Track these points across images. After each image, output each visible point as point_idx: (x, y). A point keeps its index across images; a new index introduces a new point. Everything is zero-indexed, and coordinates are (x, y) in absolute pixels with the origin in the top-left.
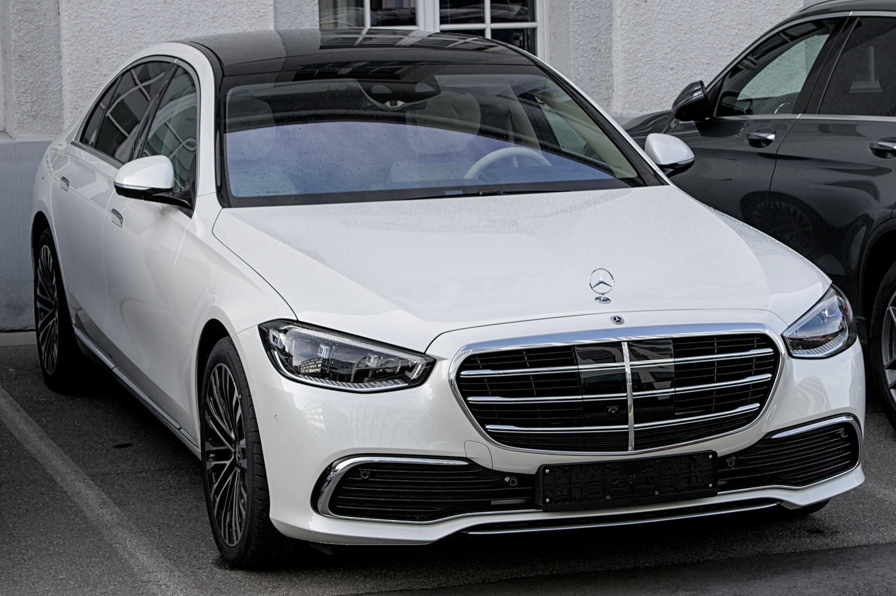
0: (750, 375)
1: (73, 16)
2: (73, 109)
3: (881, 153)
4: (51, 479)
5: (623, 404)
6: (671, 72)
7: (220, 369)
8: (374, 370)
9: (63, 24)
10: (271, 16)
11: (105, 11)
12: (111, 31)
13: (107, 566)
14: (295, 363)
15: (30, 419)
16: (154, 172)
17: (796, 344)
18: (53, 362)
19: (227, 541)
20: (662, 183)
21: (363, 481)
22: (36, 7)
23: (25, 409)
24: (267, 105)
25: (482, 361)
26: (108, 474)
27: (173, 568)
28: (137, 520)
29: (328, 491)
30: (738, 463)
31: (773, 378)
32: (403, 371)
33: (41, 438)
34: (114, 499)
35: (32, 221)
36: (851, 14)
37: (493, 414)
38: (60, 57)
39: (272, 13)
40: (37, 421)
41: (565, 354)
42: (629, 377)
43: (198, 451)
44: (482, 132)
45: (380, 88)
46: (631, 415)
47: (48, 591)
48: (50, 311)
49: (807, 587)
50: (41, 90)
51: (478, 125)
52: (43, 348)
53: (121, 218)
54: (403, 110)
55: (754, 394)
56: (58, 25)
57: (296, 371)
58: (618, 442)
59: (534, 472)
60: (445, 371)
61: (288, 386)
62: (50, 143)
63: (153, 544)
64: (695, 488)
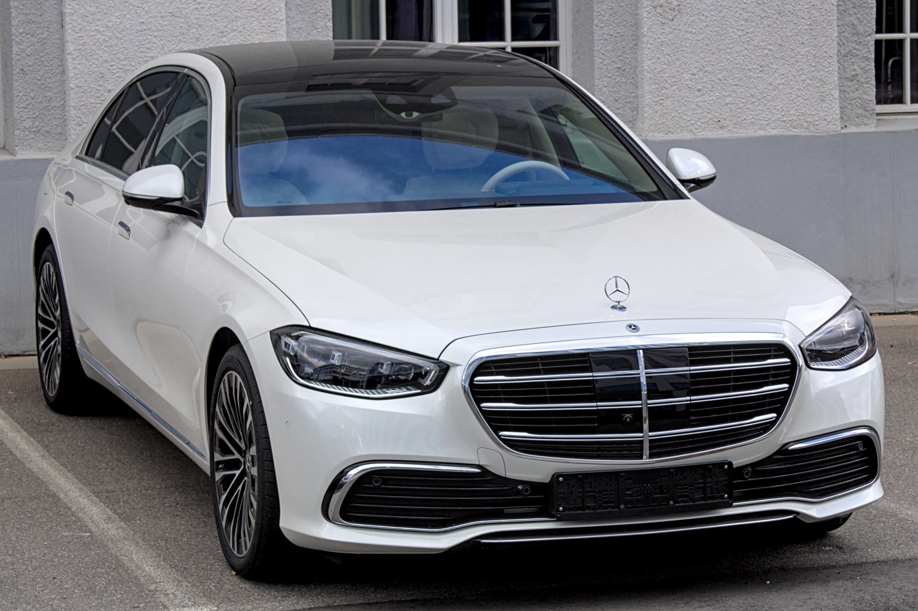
0: (767, 384)
2: (76, 125)
4: (54, 495)
6: (698, 94)
9: (68, 38)
11: (110, 24)
13: (113, 576)
15: (32, 439)
16: (167, 181)
19: (236, 552)
20: (681, 196)
21: (375, 488)
22: (39, 19)
23: (25, 430)
24: (278, 118)
26: (113, 492)
28: (144, 534)
29: (338, 498)
30: (755, 473)
32: (414, 376)
33: (43, 457)
34: (119, 515)
35: (34, 238)
37: (506, 421)
39: (284, 28)
40: (39, 442)
43: (205, 463)
44: (499, 148)
45: (395, 99)
47: (55, 599)
48: (52, 331)
50: (44, 105)
53: (128, 230)
55: (770, 404)
56: (62, 39)
57: (308, 378)
58: (633, 449)
59: (547, 480)
60: (457, 378)
61: (300, 393)
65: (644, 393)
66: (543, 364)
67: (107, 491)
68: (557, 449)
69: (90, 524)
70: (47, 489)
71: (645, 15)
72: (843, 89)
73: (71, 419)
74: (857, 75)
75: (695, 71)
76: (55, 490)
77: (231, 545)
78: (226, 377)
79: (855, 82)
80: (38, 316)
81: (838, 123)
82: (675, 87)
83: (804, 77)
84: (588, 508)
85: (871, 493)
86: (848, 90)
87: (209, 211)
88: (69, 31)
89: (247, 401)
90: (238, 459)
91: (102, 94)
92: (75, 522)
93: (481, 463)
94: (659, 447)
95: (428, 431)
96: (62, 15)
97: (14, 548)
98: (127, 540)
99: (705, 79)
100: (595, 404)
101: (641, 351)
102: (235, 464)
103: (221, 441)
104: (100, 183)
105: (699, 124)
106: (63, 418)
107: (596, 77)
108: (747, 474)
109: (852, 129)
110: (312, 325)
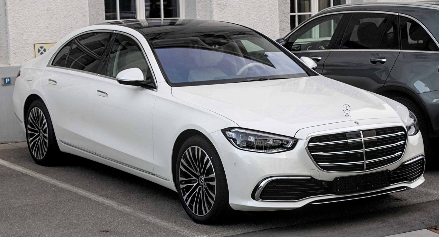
1: (12, 16)
3: (374, 62)
5: (362, 153)
9: (9, 19)
14: (238, 143)
16: (135, 74)
25: (331, 138)
31: (405, 143)
36: (349, 12)
38: (7, 33)
41: (343, 136)
42: (363, 143)
46: (365, 157)
54: (218, 48)
58: (360, 167)
64: (384, 183)
65: (364, 146)
71: (214, 7)
73: (51, 167)
87: (159, 86)
88: (9, 17)
94: (369, 166)
95: (292, 164)
96: (6, 10)
101: (361, 132)
106: (49, 168)
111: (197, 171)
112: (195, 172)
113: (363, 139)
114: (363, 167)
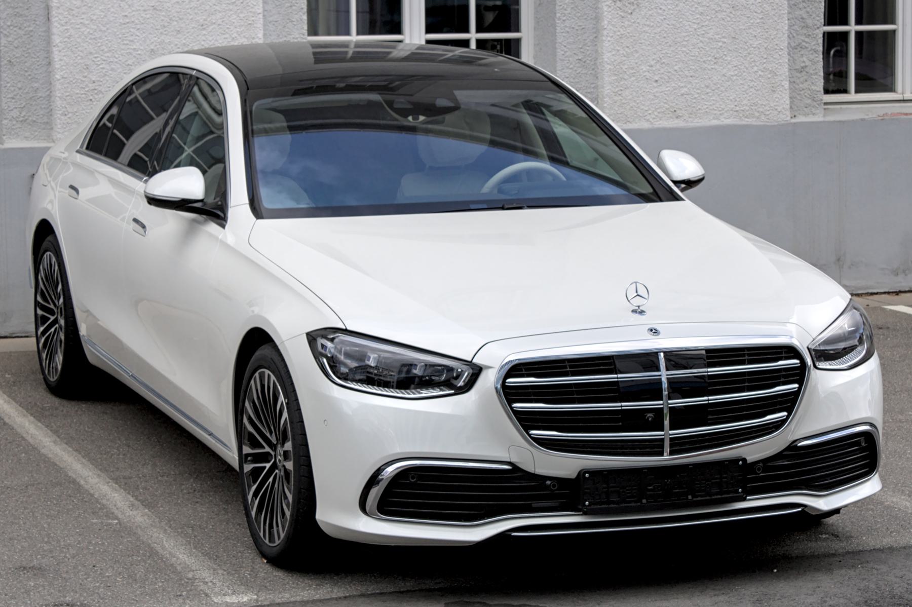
2: (62, 115)
4: (74, 482)
5: (659, 412)
6: (655, 84)
7: (262, 376)
8: (421, 377)
9: (54, 30)
10: (260, 23)
11: (94, 18)
12: (100, 38)
13: (150, 564)
15: (39, 424)
16: (186, 182)
17: (823, 354)
18: (56, 369)
19: (267, 541)
20: (676, 198)
23: (32, 415)
24: (281, 117)
26: (130, 478)
27: (215, 566)
28: (169, 521)
29: (375, 493)
31: (800, 389)
32: (446, 377)
33: (55, 442)
34: (142, 502)
39: (261, 21)
40: (47, 426)
43: (231, 456)
44: (493, 143)
46: (667, 423)
47: (99, 587)
48: (52, 318)
49: (830, 587)
50: (31, 95)
51: (488, 137)
52: (44, 356)
53: (144, 227)
54: (424, 122)
56: (48, 31)
57: (345, 379)
58: (655, 447)
60: (489, 380)
62: (48, 148)
63: (190, 543)
65: (665, 393)
66: (571, 367)
67: (125, 478)
68: (584, 447)
69: (116, 512)
70: (67, 475)
71: (605, 9)
72: (792, 80)
73: (73, 403)
74: (806, 66)
75: (653, 63)
76: (74, 476)
77: (262, 534)
78: (257, 375)
79: (804, 73)
80: (37, 304)
81: (788, 113)
82: (633, 79)
83: (756, 68)
84: (613, 502)
85: (869, 487)
86: (798, 81)
87: (231, 213)
88: (56, 24)
89: (282, 397)
90: (268, 453)
91: (87, 85)
92: (100, 509)
93: (512, 460)
94: (678, 445)
95: (462, 430)
96: (48, 8)
97: (48, 535)
98: (155, 527)
99: (662, 71)
100: (619, 404)
101: (662, 354)
102: (265, 457)
103: (250, 434)
104: (91, 172)
105: (656, 113)
106: (65, 402)
107: (558, 68)
108: (759, 469)
109: (801, 119)
110: (349, 328)
111: (271, 433)
112: (268, 435)
113: (664, 375)
114: (662, 447)
